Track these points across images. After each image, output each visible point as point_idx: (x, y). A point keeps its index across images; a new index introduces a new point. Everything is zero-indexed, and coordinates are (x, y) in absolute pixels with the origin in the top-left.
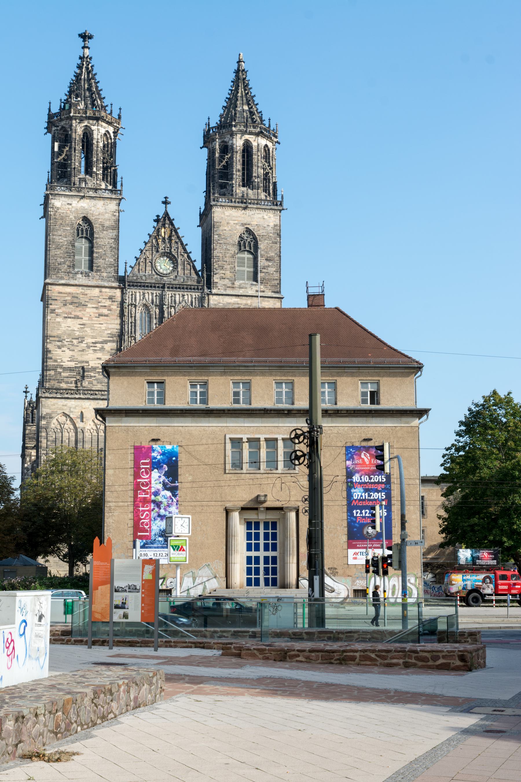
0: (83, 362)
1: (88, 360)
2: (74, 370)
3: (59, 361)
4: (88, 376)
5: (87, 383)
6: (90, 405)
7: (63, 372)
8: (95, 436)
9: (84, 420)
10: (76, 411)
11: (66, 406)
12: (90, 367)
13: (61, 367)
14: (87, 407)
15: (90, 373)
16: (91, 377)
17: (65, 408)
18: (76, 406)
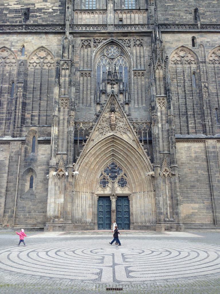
0: (29, 4)
1: (34, 3)
2: (20, 12)
3: (5, 5)
4: (34, 16)
5: (32, 22)
6: (33, 39)
7: (9, 14)
8: (37, 69)
9: (26, 53)
10: (17, 44)
11: (7, 40)
12: (36, 8)
13: (7, 9)
14: (30, 41)
15: (35, 14)
16: (36, 16)
17: (7, 42)
18: (18, 40)
